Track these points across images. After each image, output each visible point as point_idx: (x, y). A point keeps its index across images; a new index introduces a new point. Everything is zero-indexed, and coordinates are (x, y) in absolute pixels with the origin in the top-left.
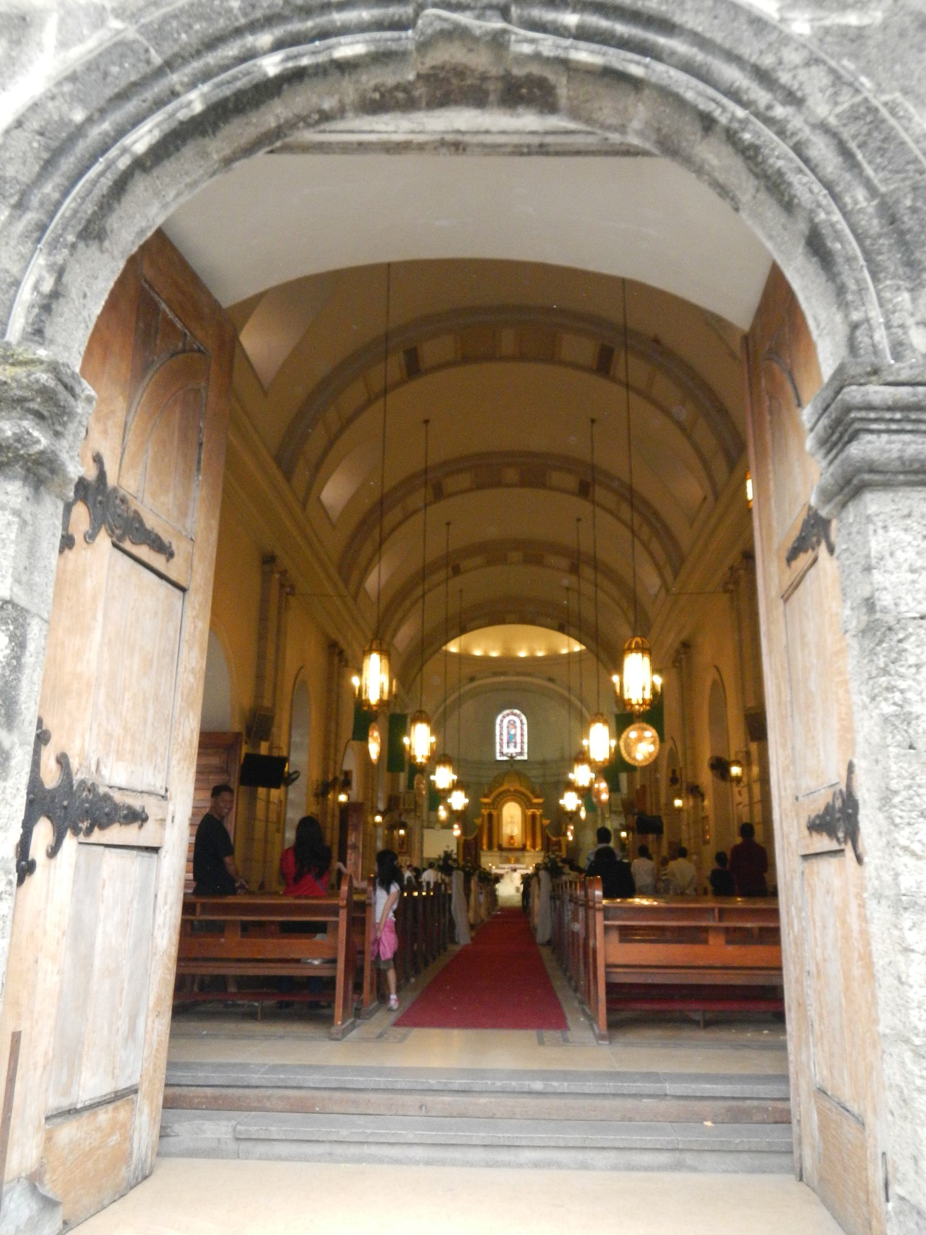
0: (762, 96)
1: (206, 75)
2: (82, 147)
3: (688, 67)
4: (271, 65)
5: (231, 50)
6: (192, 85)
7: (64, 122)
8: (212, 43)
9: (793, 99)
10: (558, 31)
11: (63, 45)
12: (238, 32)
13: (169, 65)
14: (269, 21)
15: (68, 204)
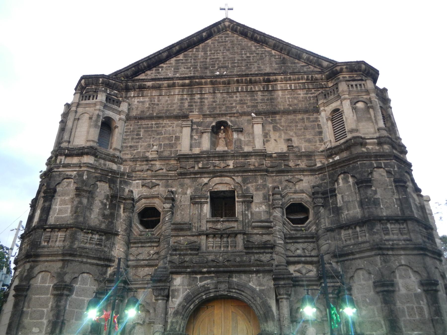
0: (252, 300)
1: (197, 299)
2: (186, 307)
3: (245, 297)
4: (204, 297)
5: (200, 295)
6: (196, 300)
7: (184, 305)
8: (198, 294)
9: (255, 301)
10: (233, 292)
11: (183, 293)
12: (201, 293)
13: (194, 297)
14: (204, 292)
15: (185, 315)
